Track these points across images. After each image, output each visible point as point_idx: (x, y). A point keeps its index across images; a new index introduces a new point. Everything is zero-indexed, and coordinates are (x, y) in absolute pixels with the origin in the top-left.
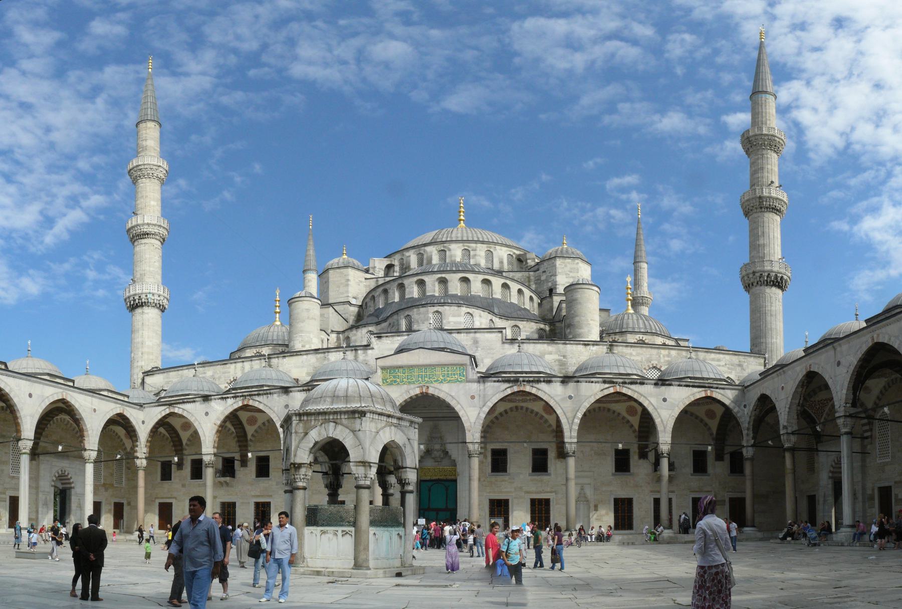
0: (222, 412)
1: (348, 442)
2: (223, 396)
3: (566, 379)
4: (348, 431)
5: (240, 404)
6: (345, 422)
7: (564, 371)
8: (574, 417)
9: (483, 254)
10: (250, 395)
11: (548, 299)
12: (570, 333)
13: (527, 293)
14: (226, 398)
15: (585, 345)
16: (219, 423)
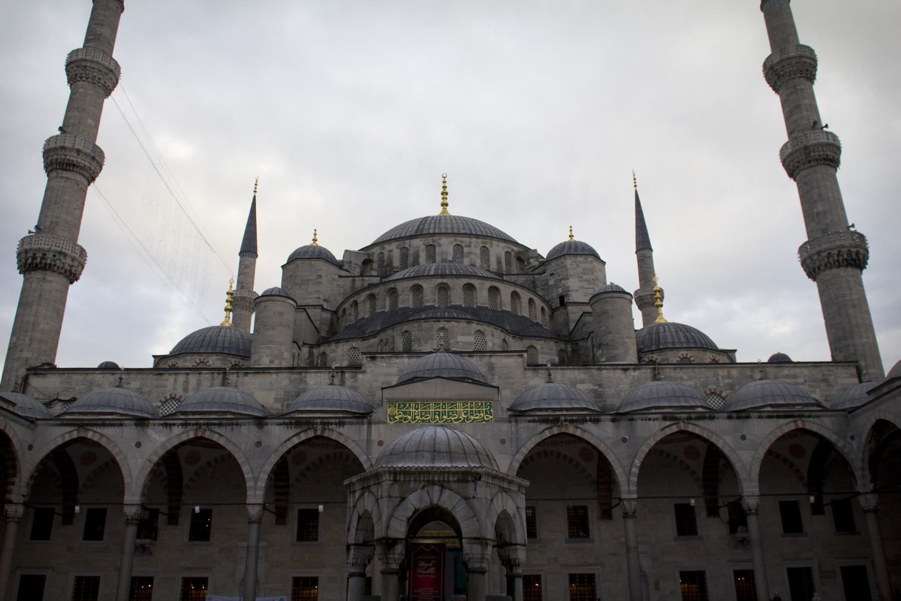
0: (163, 445)
1: (460, 512)
2: (167, 422)
3: (618, 417)
4: (459, 498)
5: (192, 435)
6: (454, 486)
7: (600, 405)
8: (632, 465)
9: (478, 251)
10: (208, 425)
11: (562, 310)
12: (602, 355)
13: (538, 303)
14: (170, 425)
15: (625, 370)
16: (155, 459)
